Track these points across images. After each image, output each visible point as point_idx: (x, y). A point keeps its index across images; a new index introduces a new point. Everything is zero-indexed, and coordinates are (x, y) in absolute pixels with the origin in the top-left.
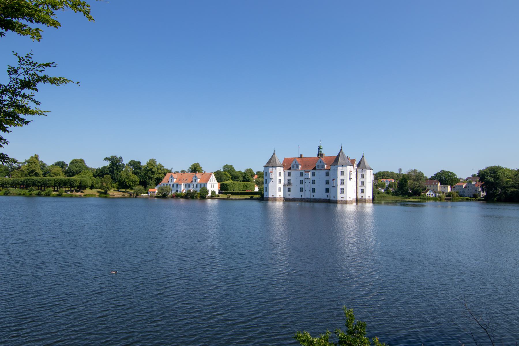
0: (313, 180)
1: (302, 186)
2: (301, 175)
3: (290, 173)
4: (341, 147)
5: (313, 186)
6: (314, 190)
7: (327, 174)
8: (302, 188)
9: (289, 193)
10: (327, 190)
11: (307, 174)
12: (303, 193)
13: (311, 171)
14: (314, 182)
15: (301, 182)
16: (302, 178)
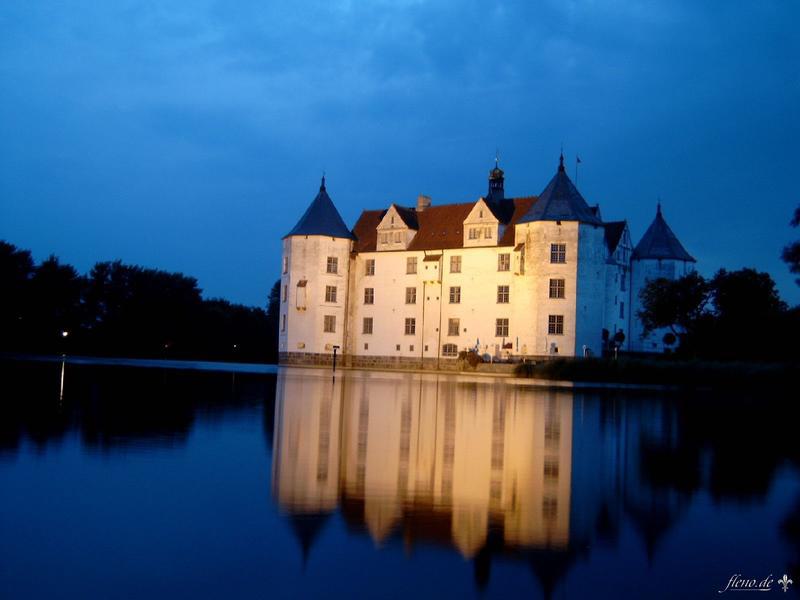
0: (452, 289)
1: (411, 311)
2: (412, 268)
3: (373, 261)
4: (562, 159)
5: (455, 311)
6: (454, 328)
7: (504, 264)
8: (413, 321)
9: (367, 338)
10: (502, 327)
11: (432, 264)
12: (411, 339)
13: (448, 254)
14: (455, 295)
15: (411, 296)
16: (411, 281)
